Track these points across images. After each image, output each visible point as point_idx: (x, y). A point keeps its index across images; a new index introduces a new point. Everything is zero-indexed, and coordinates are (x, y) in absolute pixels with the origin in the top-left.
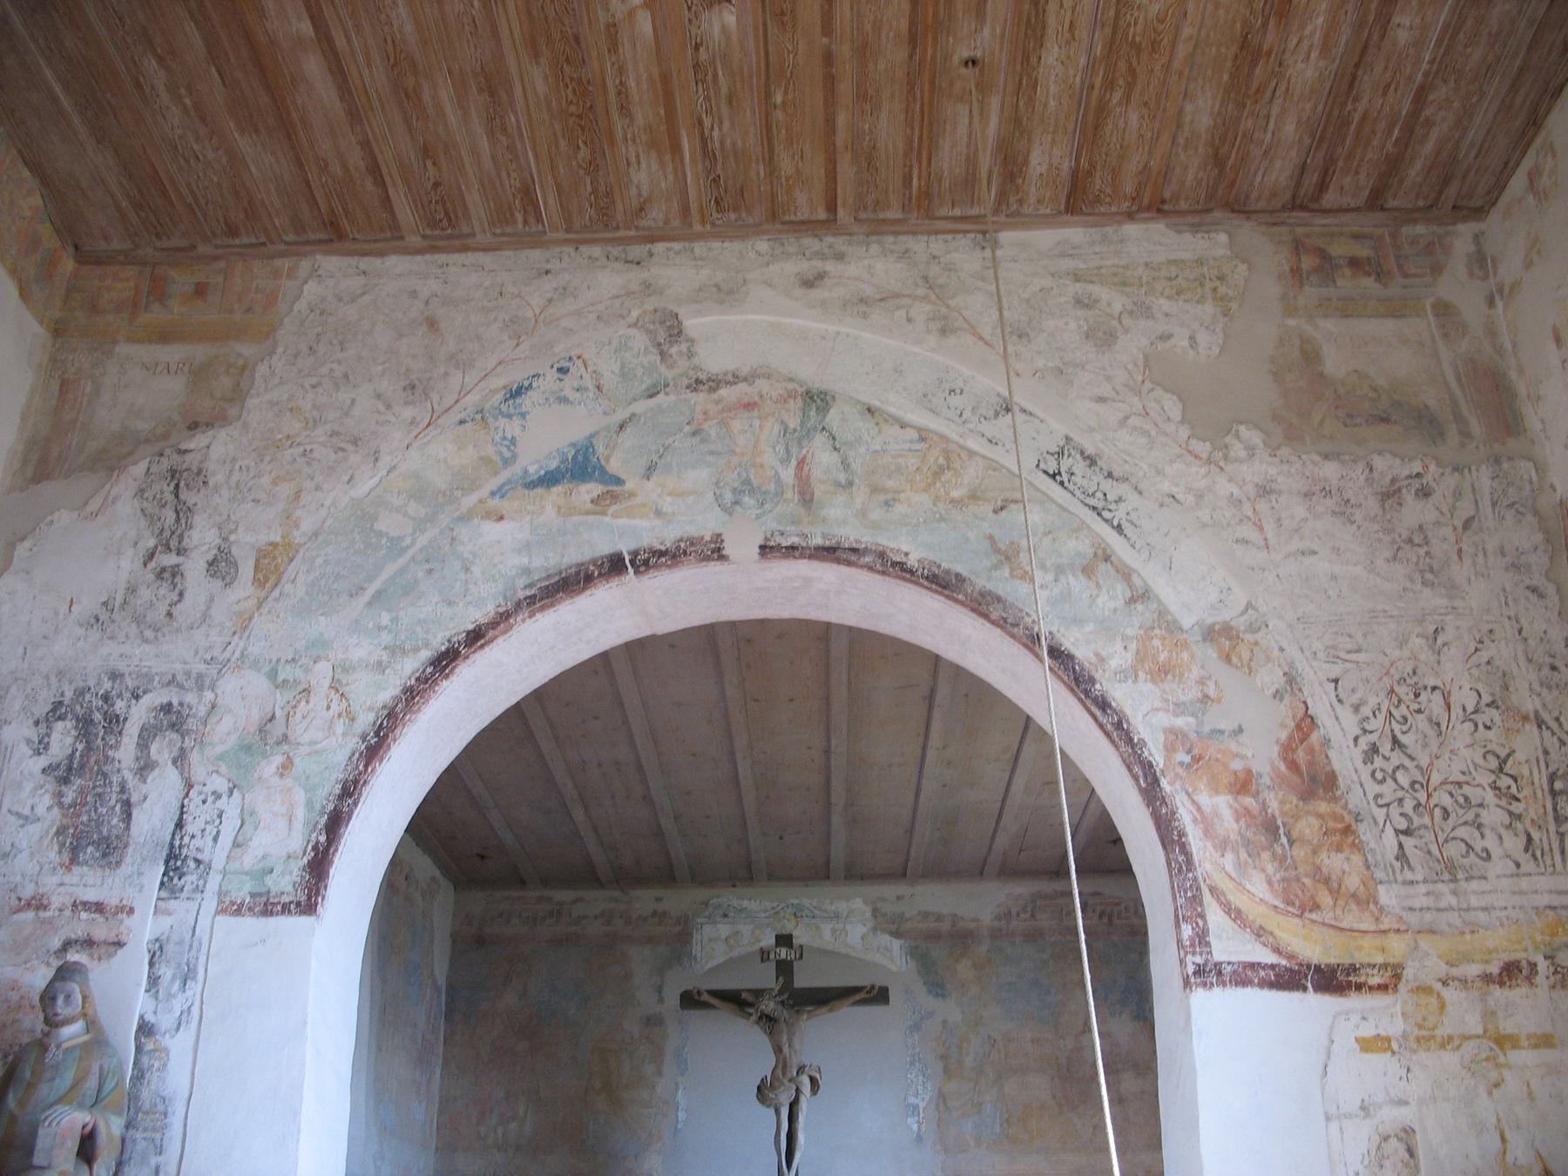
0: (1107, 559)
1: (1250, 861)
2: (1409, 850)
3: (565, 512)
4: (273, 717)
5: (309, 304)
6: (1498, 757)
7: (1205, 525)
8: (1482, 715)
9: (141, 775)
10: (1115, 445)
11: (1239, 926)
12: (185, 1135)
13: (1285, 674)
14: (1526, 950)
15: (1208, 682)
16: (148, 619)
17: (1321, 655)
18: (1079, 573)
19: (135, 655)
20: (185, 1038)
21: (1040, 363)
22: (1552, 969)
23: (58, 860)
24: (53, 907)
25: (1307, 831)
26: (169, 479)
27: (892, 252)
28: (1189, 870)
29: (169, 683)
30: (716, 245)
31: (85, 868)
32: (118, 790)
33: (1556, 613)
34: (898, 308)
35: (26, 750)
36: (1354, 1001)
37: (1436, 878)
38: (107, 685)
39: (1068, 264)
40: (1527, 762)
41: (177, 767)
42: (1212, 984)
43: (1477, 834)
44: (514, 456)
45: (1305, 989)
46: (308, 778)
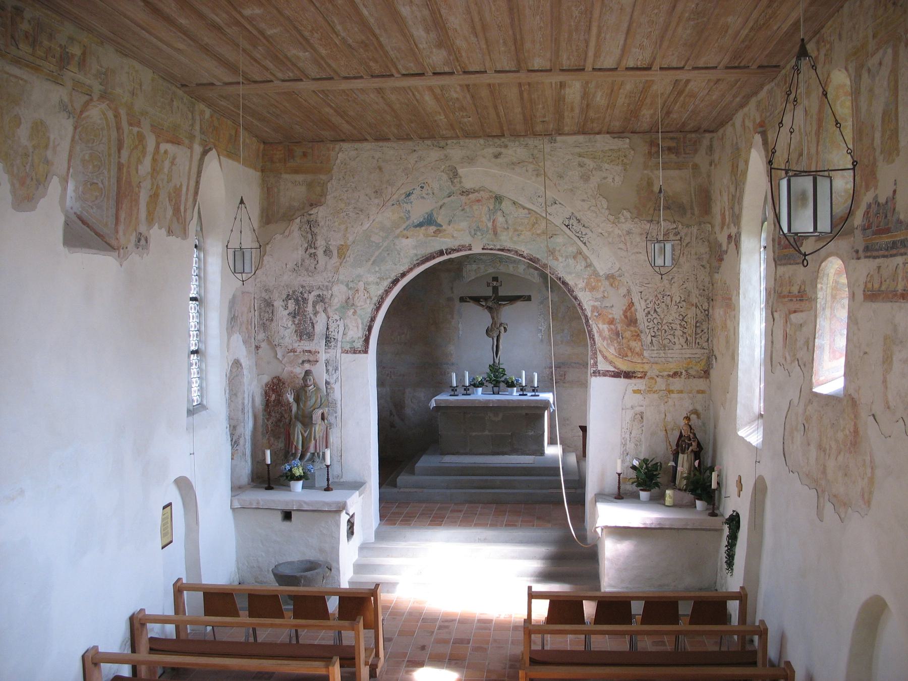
0: (581, 254)
3: (426, 236)
7: (610, 243)
17: (638, 284)
19: (308, 281)
20: (338, 384)
21: (566, 187)
27: (522, 144)
30: (467, 141)
34: (524, 166)
35: (281, 309)
36: (633, 381)
38: (301, 289)
39: (578, 150)
44: (410, 217)
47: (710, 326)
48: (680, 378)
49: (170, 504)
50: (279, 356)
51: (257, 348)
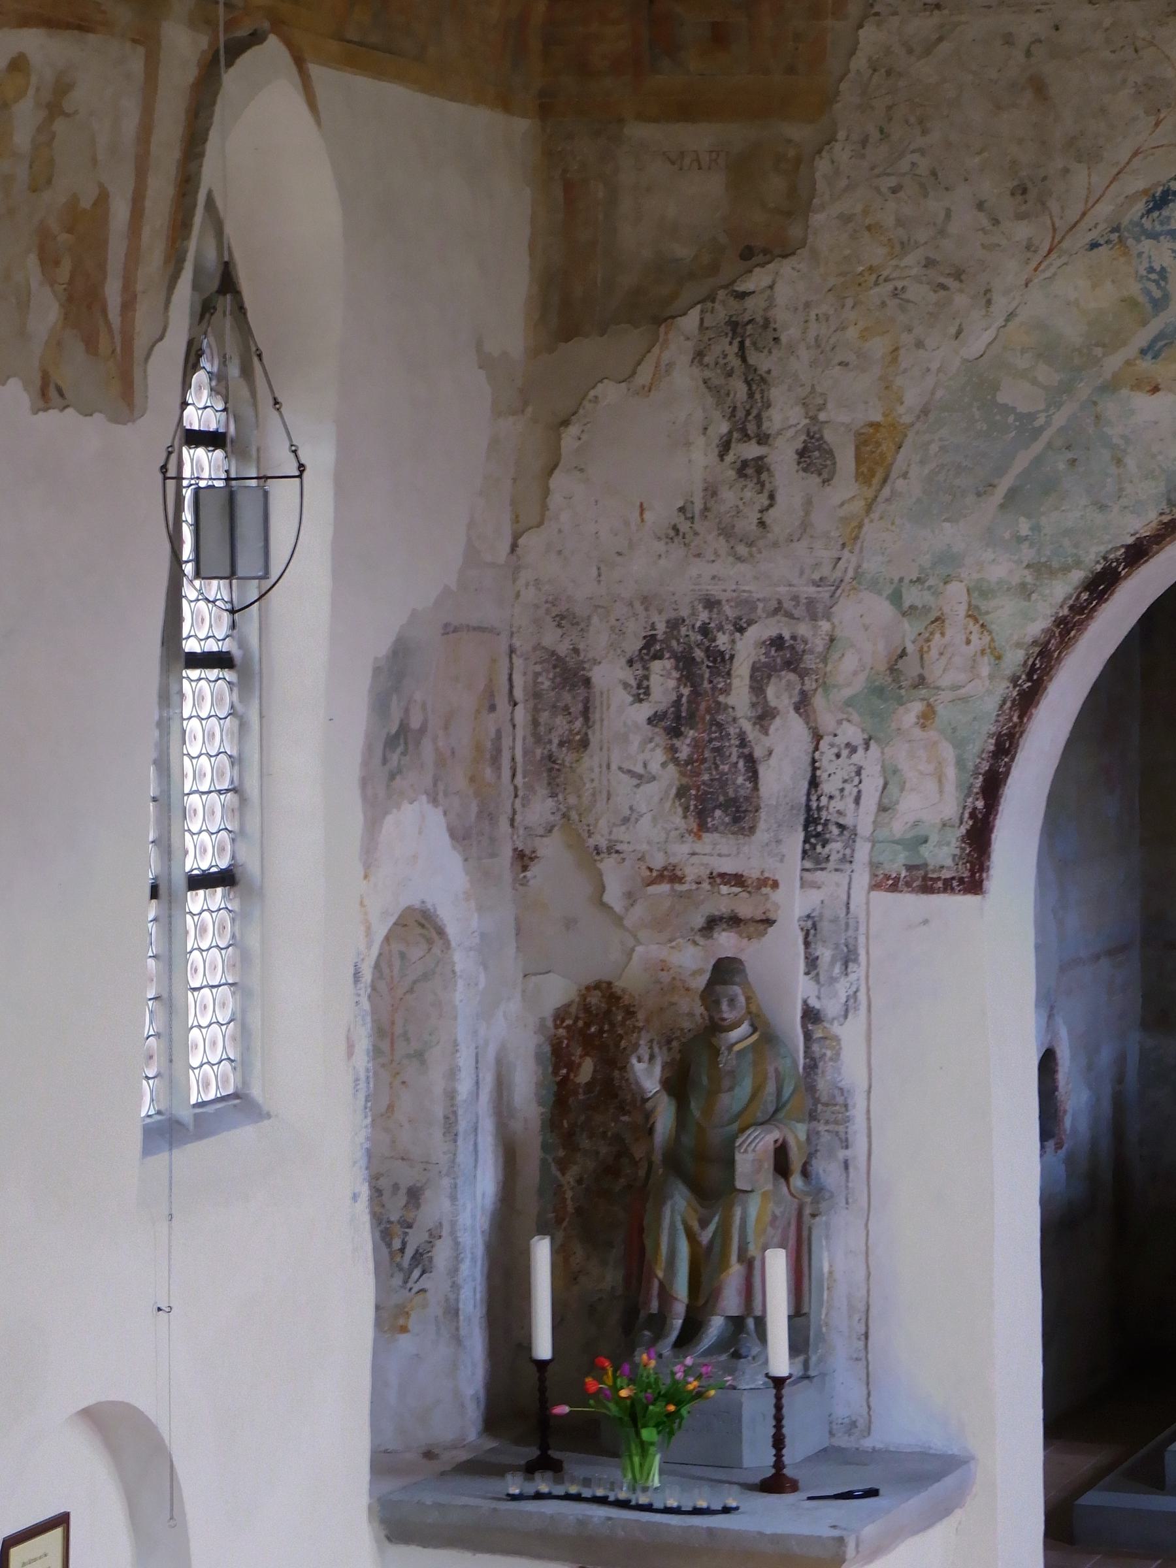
4: (903, 654)
5: (870, 59)
9: (762, 726)
12: (869, 1128)
16: (736, 530)
23: (685, 826)
24: (688, 879)
26: (730, 335)
29: (776, 611)
31: (716, 835)
32: (738, 743)
38: (704, 616)
41: (800, 715)
44: (1166, 297)
46: (954, 730)
49: (62, 1521)
50: (614, 896)
51: (523, 859)
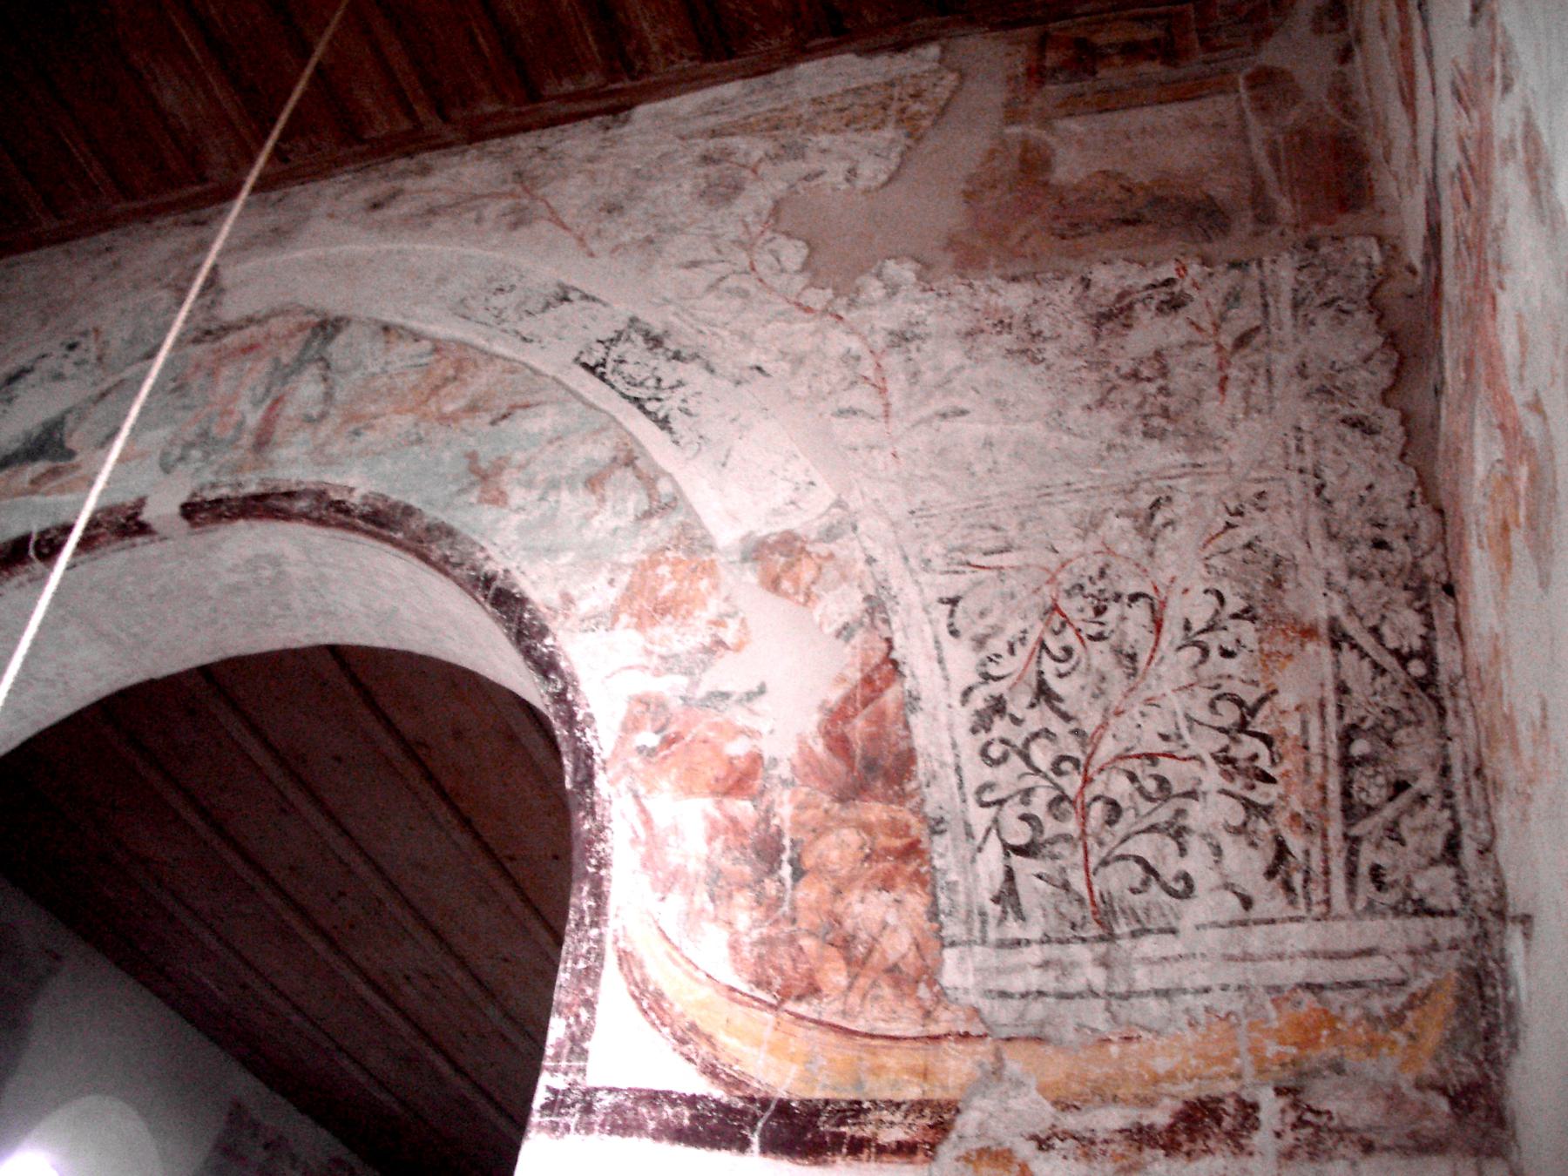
0: (630, 462)
1: (710, 907)
2: (1025, 883)
6: (1240, 703)
8: (1223, 634)
10: (692, 315)
11: (653, 1024)
13: (868, 598)
14: (1237, 1076)
15: (729, 621)
17: (938, 563)
18: (580, 485)
22: (1291, 1116)
25: (834, 855)
28: (594, 924)
33: (1394, 454)
37: (1069, 933)
40: (1297, 708)
42: (567, 1128)
43: (1171, 846)
45: (743, 1145)
47: (1454, 749)
48: (1240, 1149)
